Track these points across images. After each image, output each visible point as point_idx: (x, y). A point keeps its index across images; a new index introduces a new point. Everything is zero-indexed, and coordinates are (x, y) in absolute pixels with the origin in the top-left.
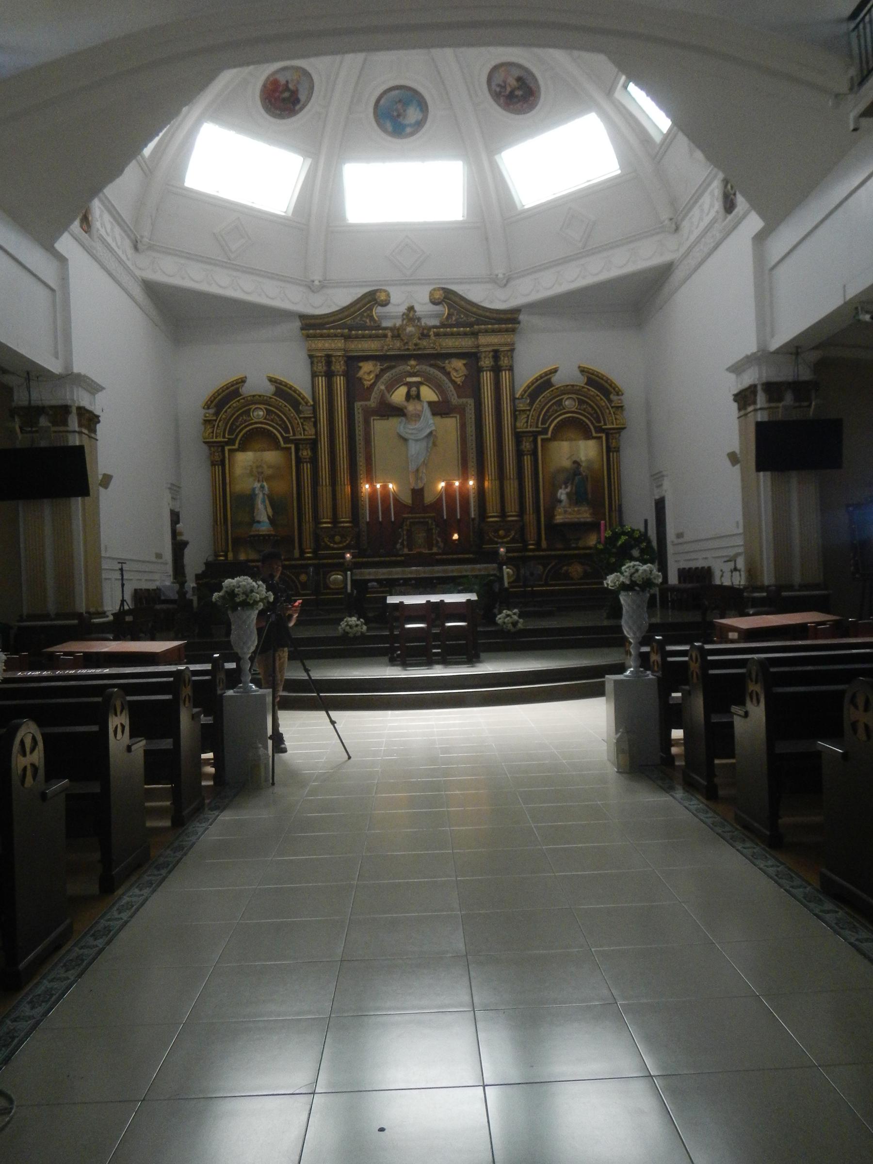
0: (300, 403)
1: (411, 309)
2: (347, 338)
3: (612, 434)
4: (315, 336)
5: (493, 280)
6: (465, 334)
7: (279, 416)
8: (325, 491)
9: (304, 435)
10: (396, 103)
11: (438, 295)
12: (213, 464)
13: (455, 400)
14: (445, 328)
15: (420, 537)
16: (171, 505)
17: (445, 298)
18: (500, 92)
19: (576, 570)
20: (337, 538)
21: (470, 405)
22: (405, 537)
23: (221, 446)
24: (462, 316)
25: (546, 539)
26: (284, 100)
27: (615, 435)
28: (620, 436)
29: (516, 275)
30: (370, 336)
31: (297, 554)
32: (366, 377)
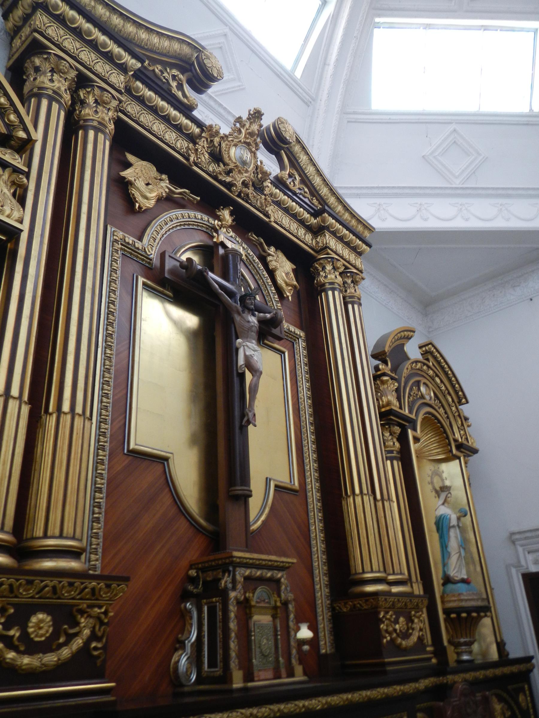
6: (302, 222)
24: (306, 190)
30: (166, 119)
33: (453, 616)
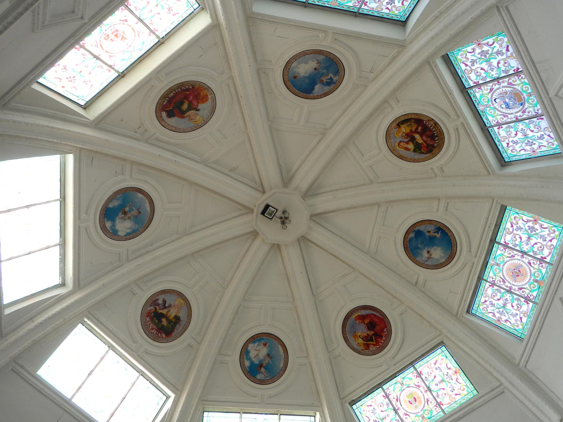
10: (138, 209)
18: (158, 305)
26: (182, 103)
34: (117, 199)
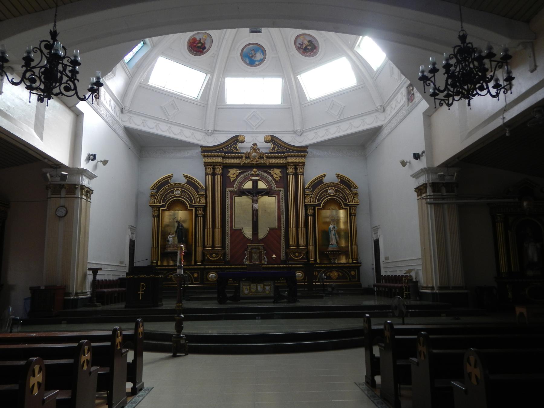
0: (199, 188)
1: (255, 144)
2: (223, 157)
3: (352, 207)
4: (208, 156)
5: (295, 133)
6: (281, 157)
7: (188, 194)
8: (209, 232)
9: (200, 203)
10: (251, 50)
11: (269, 138)
12: (154, 217)
13: (275, 188)
14: (271, 154)
15: (255, 256)
16: (130, 237)
17: (271, 140)
18: (300, 47)
19: (335, 274)
20: (214, 255)
21: (283, 191)
22: (248, 256)
23: (159, 208)
24: (280, 149)
25: (319, 259)
26: (198, 47)
27: (353, 207)
28: (356, 208)
29: (306, 131)
31: (193, 263)
32: (232, 176)
33: (330, 252)
34: (245, 60)
